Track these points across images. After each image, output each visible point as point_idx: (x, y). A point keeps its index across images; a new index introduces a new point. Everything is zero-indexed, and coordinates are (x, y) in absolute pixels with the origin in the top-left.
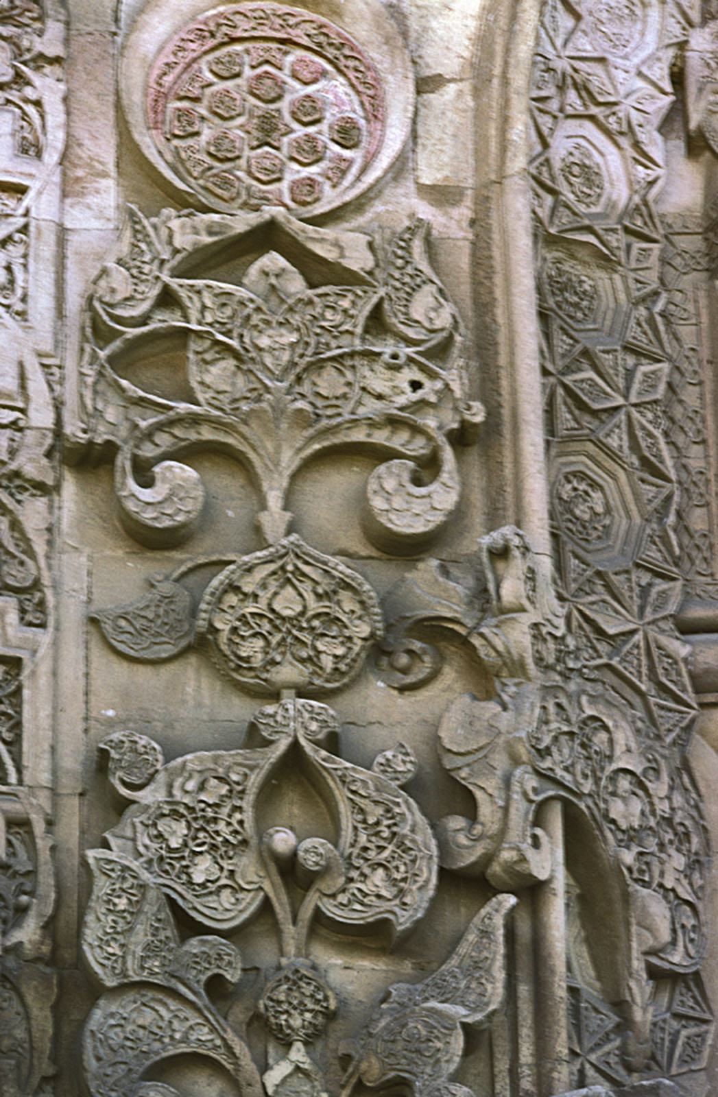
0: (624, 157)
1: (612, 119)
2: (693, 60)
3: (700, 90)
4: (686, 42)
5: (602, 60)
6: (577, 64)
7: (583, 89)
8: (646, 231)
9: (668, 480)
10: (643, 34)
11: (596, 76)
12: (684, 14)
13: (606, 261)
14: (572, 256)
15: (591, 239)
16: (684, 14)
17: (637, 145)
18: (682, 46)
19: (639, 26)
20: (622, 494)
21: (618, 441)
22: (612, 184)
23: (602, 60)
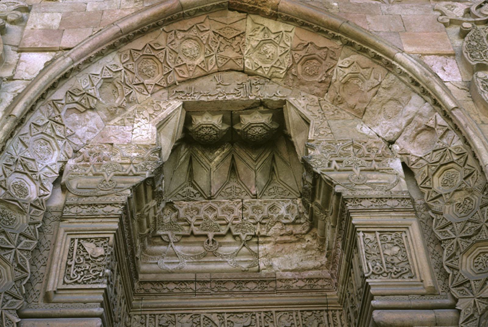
0: (37, 187)
1: (34, 176)
2: (68, 166)
3: (67, 173)
4: (67, 162)
5: (33, 160)
6: (23, 159)
7: (25, 166)
8: (40, 207)
9: (27, 272)
10: (52, 158)
11: (31, 164)
12: (67, 154)
13: (22, 211)
14: (9, 208)
15: (16, 204)
16: (67, 154)
17: (42, 184)
18: (65, 162)
19: (51, 156)
20: (7, 273)
21: (10, 257)
22: (31, 193)
23: (33, 160)
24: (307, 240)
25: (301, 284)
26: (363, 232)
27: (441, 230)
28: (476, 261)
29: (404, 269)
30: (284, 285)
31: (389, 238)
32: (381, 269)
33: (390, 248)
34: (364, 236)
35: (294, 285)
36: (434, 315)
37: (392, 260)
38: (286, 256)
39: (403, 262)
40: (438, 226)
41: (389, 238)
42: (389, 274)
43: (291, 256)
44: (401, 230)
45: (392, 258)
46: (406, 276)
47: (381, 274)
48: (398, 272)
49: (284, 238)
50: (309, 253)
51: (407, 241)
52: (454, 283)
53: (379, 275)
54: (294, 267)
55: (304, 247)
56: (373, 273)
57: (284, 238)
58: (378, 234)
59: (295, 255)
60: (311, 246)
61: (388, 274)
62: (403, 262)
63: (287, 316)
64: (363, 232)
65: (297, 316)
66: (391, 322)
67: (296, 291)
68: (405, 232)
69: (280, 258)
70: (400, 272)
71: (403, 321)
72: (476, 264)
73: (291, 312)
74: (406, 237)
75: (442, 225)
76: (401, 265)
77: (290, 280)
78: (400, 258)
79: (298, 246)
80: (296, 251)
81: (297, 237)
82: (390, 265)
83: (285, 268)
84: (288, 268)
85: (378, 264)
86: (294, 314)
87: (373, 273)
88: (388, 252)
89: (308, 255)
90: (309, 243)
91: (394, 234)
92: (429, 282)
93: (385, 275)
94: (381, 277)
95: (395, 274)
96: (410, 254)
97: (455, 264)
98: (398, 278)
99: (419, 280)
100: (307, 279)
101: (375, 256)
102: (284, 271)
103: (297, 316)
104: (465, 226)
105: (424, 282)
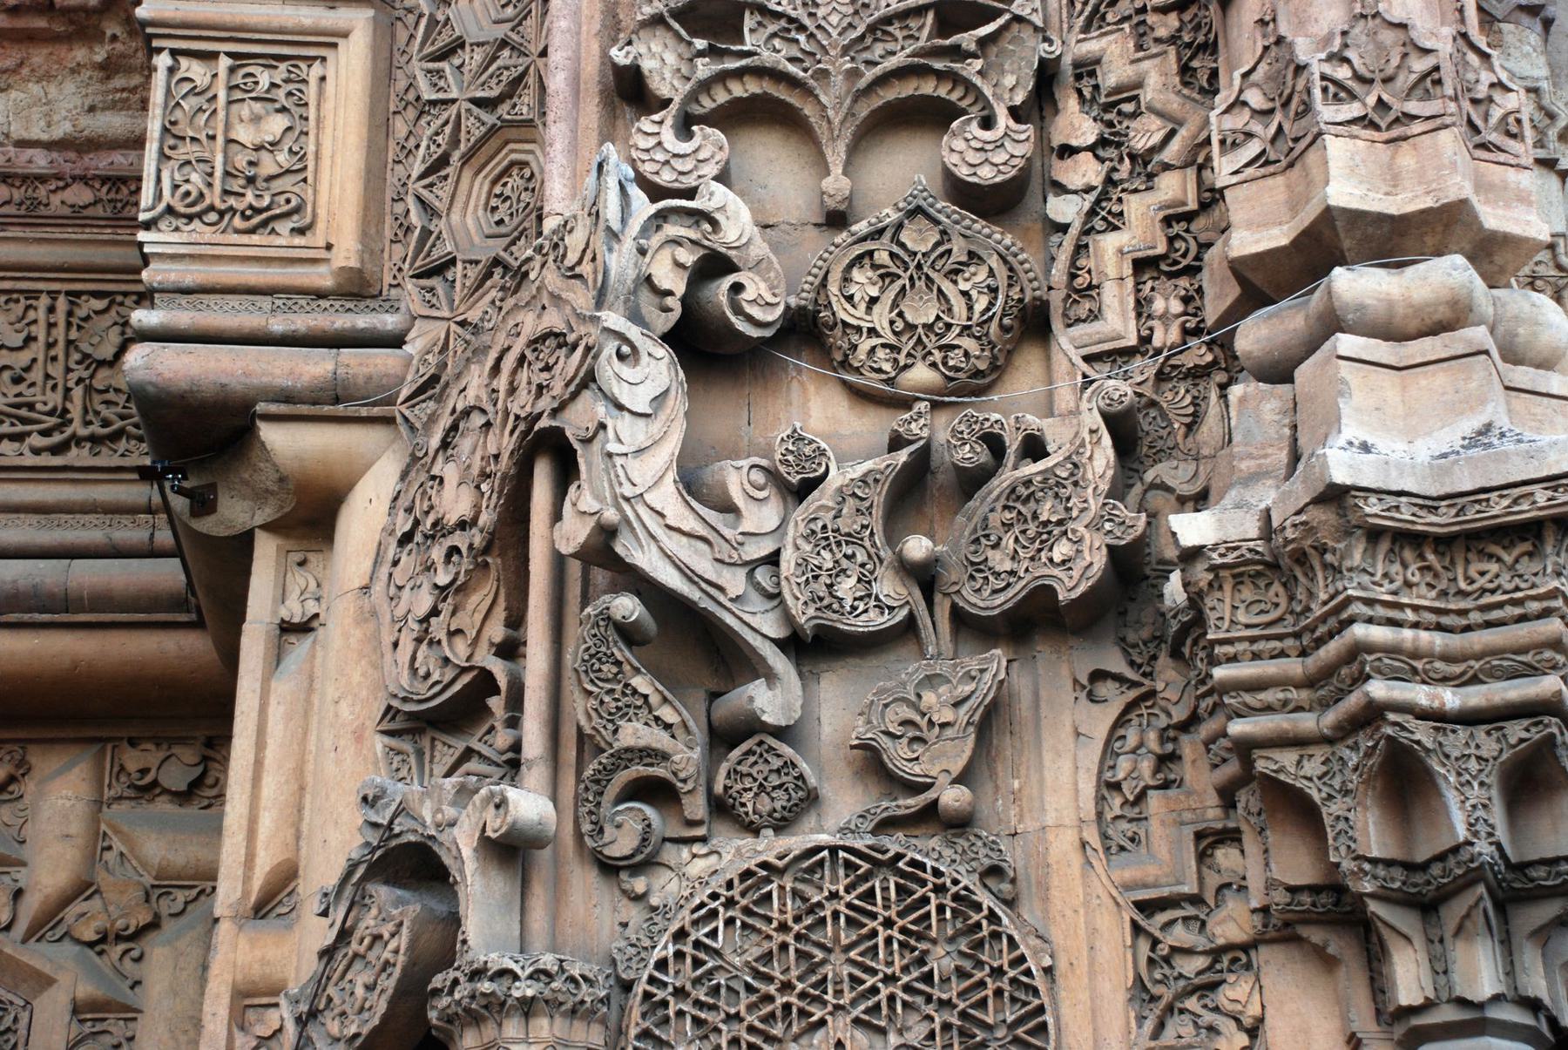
24: (109, 33)
25: (80, 195)
26: (174, 53)
27: (431, 65)
28: (497, 190)
29: (282, 199)
30: (17, 195)
31: (264, 78)
32: (202, 195)
33: (256, 119)
34: (171, 71)
35: (55, 200)
36: (330, 367)
37: (251, 163)
38: (35, 88)
39: (288, 171)
40: (428, 49)
41: (264, 78)
42: (227, 218)
43: (53, 90)
44: (312, 52)
45: (253, 157)
46: (284, 227)
47: (199, 216)
48: (258, 211)
49: (22, 23)
50: (118, 82)
51: (321, 93)
52: (418, 263)
53: (190, 218)
54: (58, 133)
55: (99, 58)
56: (170, 210)
57: (22, 23)
58: (224, 62)
59: (70, 87)
60: (123, 56)
61: (222, 214)
62: (288, 171)
63: (18, 309)
64: (174, 53)
65: (51, 310)
66: (184, 386)
67: (58, 221)
68: (324, 59)
69: (14, 94)
70: (268, 208)
71: (223, 386)
72: (494, 202)
73: (33, 295)
74: (323, 79)
75: (439, 44)
76: (277, 185)
77: (42, 179)
78: (283, 157)
79: (80, 54)
80: (73, 71)
81: (72, 22)
82: (235, 185)
83: (26, 135)
84: (36, 133)
85: (195, 177)
86: (44, 301)
87: (170, 210)
88: (243, 134)
89: (117, 90)
90: (119, 47)
91: (283, 66)
92: (347, 253)
93: (213, 217)
94: (196, 224)
95: (246, 218)
96: (318, 144)
97: (439, 196)
98: (252, 231)
99: (322, 243)
100: (105, 180)
101: (196, 147)
102: (23, 144)
103: (51, 310)
104: (494, 58)
105: (334, 250)
